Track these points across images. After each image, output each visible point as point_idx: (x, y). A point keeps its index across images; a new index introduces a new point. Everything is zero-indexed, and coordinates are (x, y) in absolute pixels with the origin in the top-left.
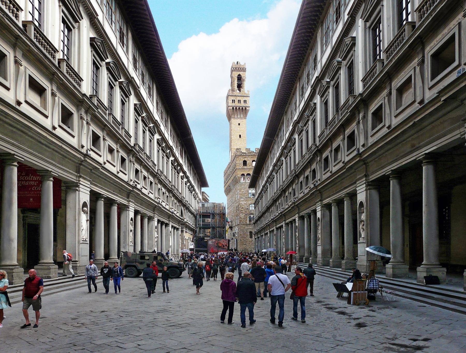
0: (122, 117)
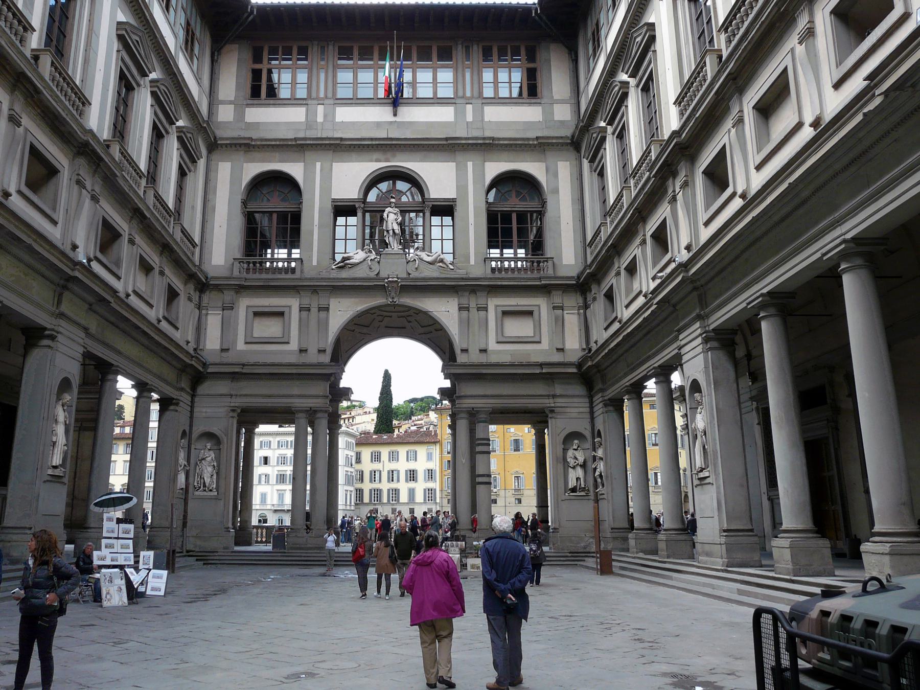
0: (179, 199)
